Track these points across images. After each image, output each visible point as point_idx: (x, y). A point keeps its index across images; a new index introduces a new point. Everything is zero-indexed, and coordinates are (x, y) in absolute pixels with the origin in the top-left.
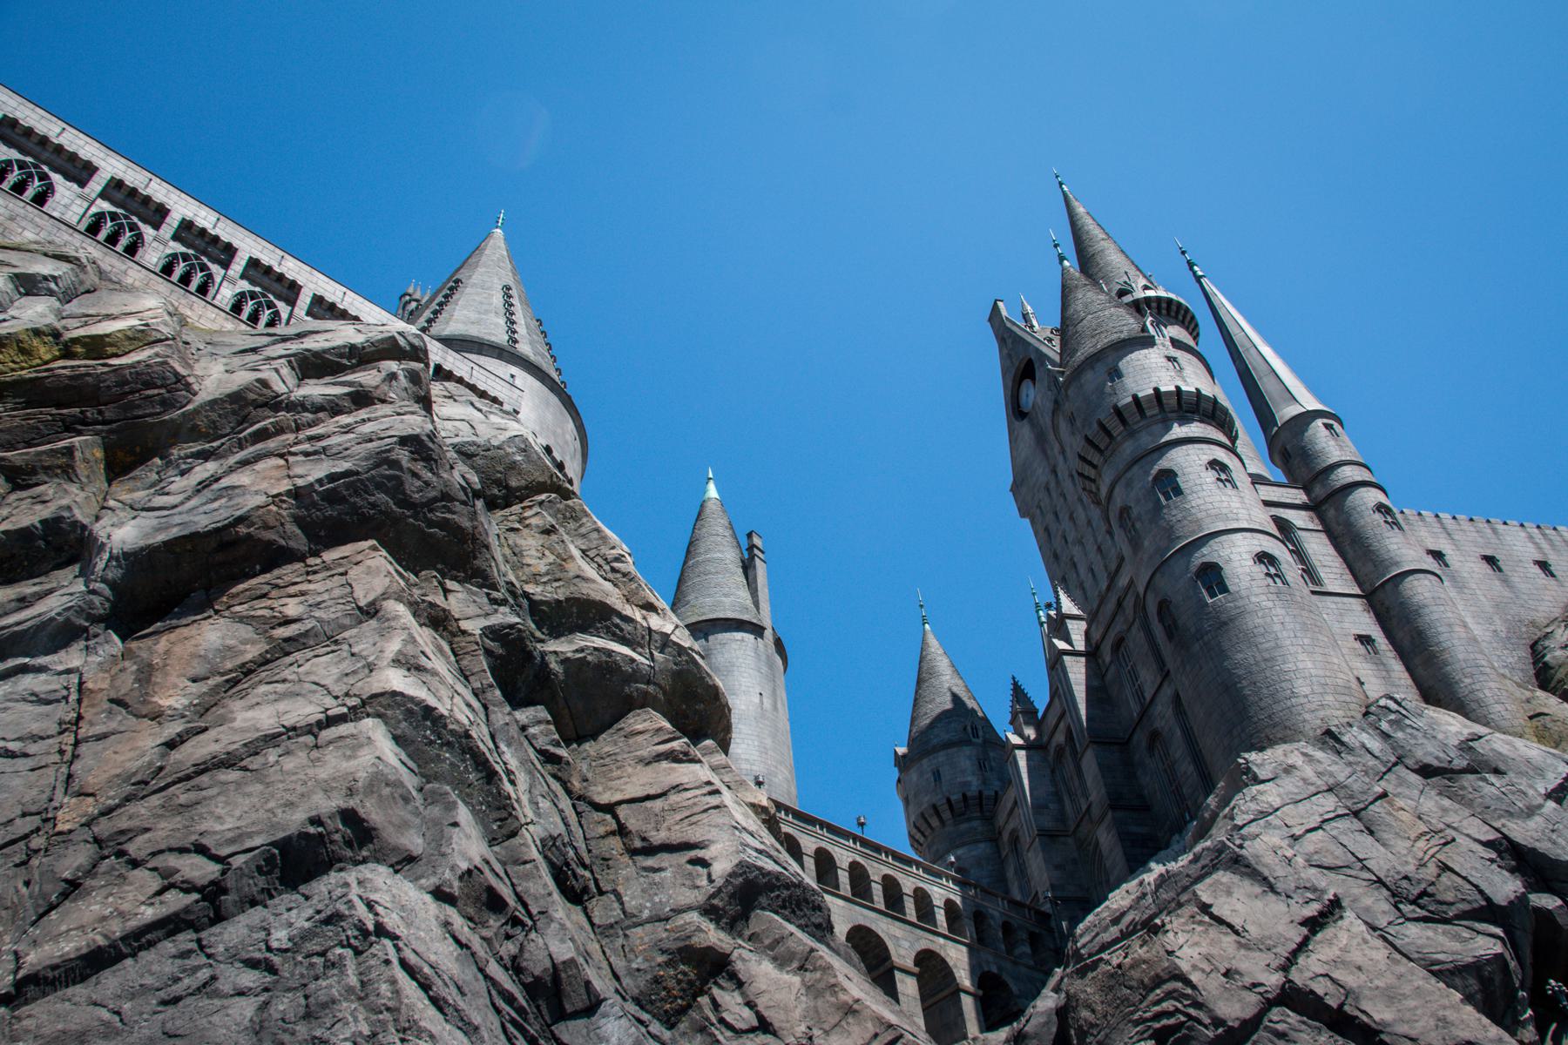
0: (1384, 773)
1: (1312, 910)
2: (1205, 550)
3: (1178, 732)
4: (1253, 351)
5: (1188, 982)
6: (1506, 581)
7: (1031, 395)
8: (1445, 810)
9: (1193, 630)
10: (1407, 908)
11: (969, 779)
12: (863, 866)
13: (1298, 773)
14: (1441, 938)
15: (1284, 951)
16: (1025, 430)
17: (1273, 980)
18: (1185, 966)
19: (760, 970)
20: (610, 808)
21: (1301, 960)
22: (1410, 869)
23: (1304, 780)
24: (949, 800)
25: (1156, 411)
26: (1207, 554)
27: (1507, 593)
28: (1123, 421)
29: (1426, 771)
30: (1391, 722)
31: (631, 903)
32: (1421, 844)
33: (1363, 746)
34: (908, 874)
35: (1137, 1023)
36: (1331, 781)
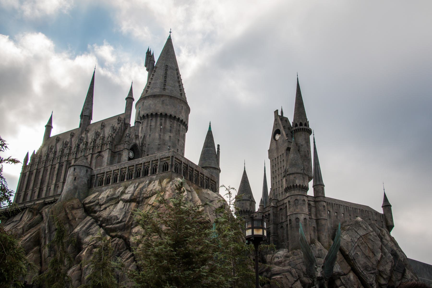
1: (296, 279)
3: (286, 230)
5: (283, 284)
7: (277, 137)
9: (293, 226)
10: (305, 275)
11: (248, 207)
14: (307, 280)
15: (292, 283)
17: (291, 286)
18: (283, 283)
21: (293, 285)
23: (300, 256)
24: (244, 210)
28: (294, 187)
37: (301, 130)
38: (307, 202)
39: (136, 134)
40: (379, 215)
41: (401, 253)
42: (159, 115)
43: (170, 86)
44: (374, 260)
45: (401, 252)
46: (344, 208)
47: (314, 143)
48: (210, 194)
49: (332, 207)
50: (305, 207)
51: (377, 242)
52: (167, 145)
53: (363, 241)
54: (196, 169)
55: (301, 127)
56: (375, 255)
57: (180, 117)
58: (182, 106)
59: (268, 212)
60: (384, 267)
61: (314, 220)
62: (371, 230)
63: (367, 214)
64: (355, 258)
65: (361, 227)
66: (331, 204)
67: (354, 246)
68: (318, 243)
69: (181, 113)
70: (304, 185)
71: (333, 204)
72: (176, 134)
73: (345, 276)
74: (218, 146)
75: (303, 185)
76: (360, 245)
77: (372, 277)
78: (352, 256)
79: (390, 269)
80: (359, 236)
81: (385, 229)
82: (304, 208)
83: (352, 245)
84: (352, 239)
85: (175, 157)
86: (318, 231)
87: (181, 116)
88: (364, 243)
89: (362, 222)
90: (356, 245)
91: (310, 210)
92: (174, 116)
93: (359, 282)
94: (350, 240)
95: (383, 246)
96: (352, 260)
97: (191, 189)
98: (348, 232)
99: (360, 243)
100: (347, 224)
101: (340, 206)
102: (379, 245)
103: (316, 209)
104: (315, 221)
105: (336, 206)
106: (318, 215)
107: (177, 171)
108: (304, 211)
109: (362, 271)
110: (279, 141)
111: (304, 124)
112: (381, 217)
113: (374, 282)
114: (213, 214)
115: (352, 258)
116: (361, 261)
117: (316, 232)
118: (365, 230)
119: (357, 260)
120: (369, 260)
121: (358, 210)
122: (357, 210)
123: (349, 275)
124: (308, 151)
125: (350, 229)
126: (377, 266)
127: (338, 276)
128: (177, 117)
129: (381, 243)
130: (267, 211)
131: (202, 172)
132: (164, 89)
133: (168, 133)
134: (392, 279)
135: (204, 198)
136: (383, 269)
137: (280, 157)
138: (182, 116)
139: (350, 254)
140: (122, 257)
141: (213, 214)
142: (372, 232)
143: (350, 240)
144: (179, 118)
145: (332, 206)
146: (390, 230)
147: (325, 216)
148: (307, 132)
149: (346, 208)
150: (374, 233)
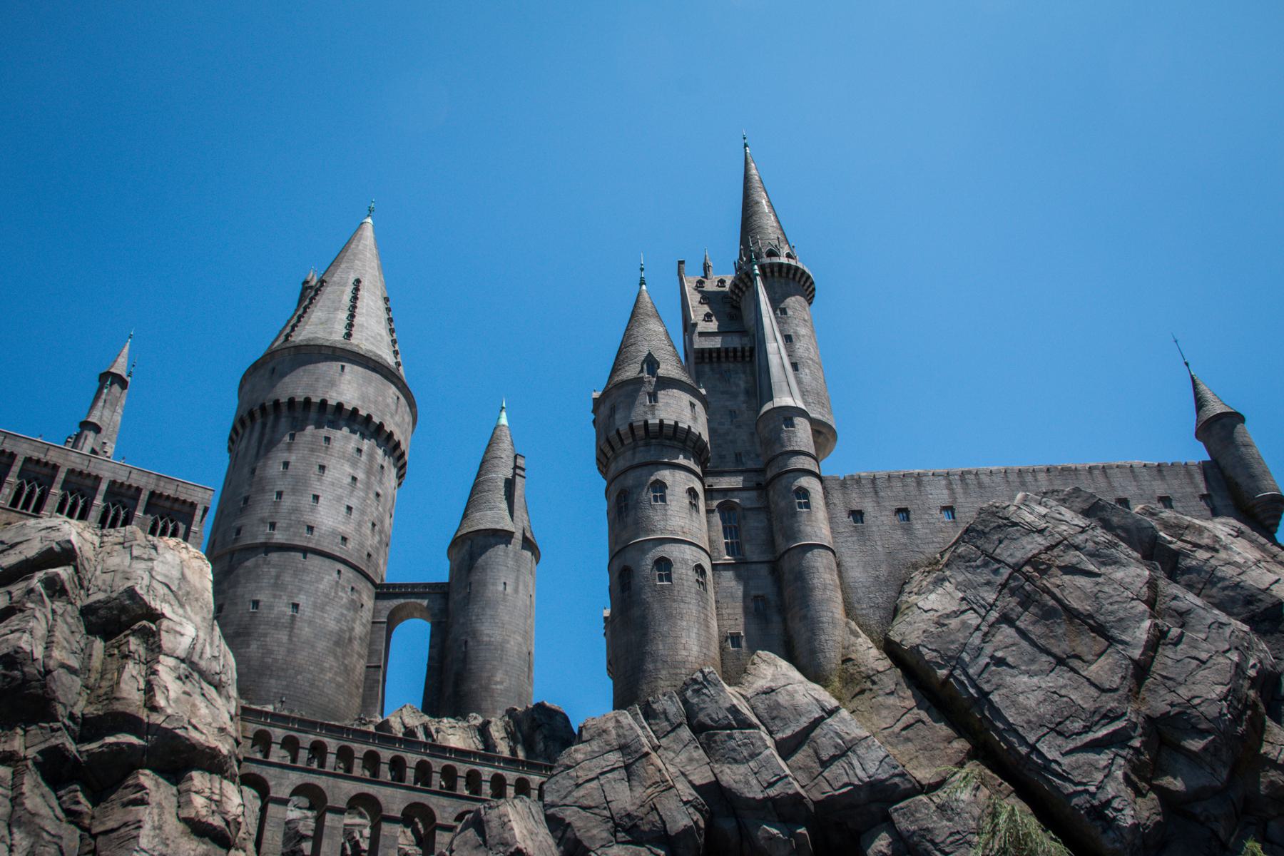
0: (669, 732)
6: (908, 530)
12: (429, 763)
13: (605, 736)
22: (630, 808)
30: (694, 691)
32: (649, 791)
33: (665, 712)
36: (623, 741)
42: (258, 411)
49: (876, 493)
57: (327, 397)
60: (1182, 691)
61: (759, 566)
62: (1076, 522)
64: (986, 687)
65: (1015, 524)
67: (978, 628)
70: (650, 422)
75: (646, 422)
77: (1103, 763)
79: (1219, 690)
80: (1006, 572)
84: (970, 594)
86: (782, 610)
90: (994, 615)
92: (302, 399)
94: (953, 606)
103: (769, 520)
104: (764, 570)
105: (897, 484)
106: (779, 540)
108: (660, 525)
109: (1033, 748)
113: (1115, 788)
117: (776, 619)
118: (1041, 532)
119: (1003, 691)
120: (1076, 672)
125: (959, 556)
126: (1134, 695)
127: (874, 808)
128: (316, 400)
129: (1147, 573)
133: (280, 454)
134: (1265, 748)
136: (1177, 700)
139: (957, 672)
142: (1083, 531)
144: (324, 403)
146: (1268, 522)
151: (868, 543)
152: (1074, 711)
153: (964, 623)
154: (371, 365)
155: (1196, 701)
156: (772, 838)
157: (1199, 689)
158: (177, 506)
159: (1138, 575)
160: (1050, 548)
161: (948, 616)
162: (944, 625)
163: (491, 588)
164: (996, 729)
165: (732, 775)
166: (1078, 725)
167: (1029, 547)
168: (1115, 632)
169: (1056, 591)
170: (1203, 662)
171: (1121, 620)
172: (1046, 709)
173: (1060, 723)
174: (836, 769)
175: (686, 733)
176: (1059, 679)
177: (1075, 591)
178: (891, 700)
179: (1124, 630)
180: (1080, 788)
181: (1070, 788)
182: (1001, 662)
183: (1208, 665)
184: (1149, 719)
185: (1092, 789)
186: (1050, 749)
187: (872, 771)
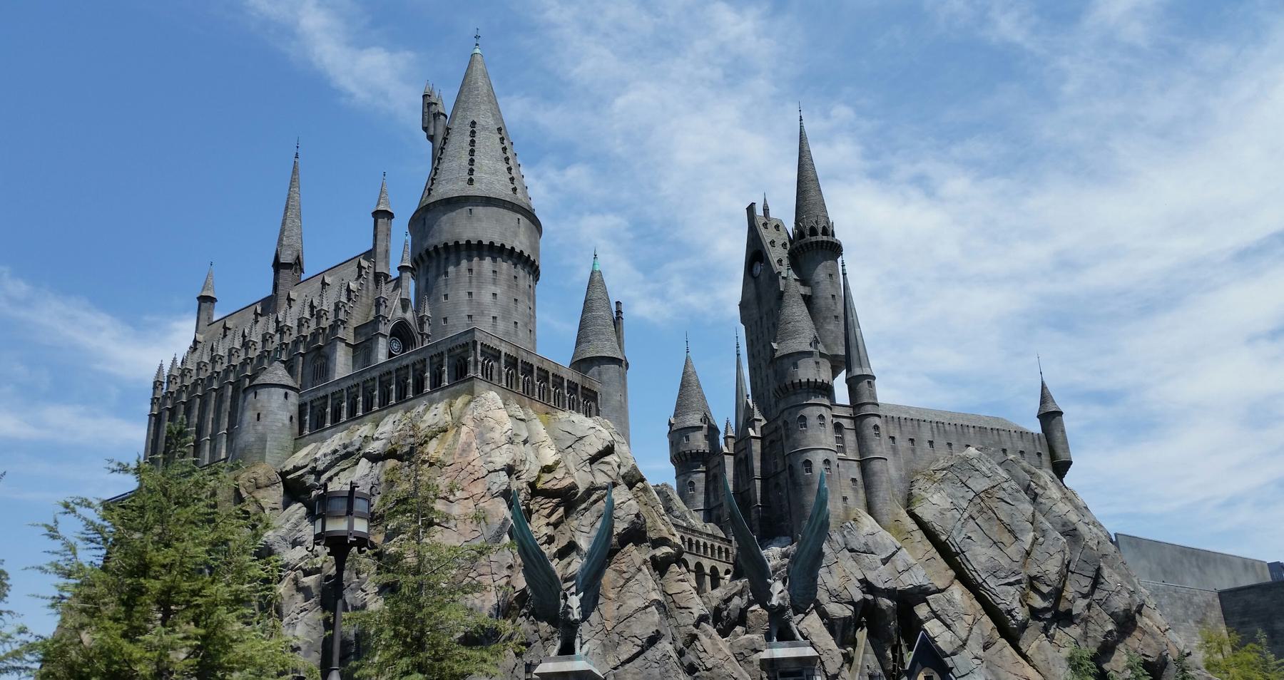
2: (808, 454)
4: (853, 330)
6: (913, 451)
8: (852, 566)
11: (700, 444)
14: (838, 609)
16: (752, 285)
19: (702, 637)
20: (671, 595)
21: (801, 623)
22: (835, 587)
25: (806, 387)
26: (809, 456)
27: (913, 457)
29: (852, 550)
31: (679, 622)
32: (842, 580)
34: (694, 536)
35: (763, 629)
37: (814, 245)
38: (829, 418)
39: (402, 297)
40: (1031, 438)
41: (1090, 529)
42: (464, 247)
43: (486, 174)
44: (1014, 551)
45: (1091, 526)
46: (932, 428)
47: (844, 274)
48: (576, 421)
49: (900, 428)
50: (825, 432)
51: (1021, 507)
52: (489, 315)
53: (982, 504)
54: (541, 366)
55: (814, 239)
56: (1016, 538)
58: (519, 219)
59: (744, 451)
63: (997, 437)
66: (896, 420)
68: (866, 517)
69: (516, 235)
71: (902, 421)
72: (509, 287)
73: (939, 595)
74: (618, 303)
75: (816, 380)
76: (975, 515)
77: (1012, 593)
78: (955, 544)
79: (1057, 569)
81: (1047, 473)
82: (823, 436)
83: (956, 518)
84: (955, 502)
85: (482, 344)
87: (518, 243)
88: (985, 510)
89: (979, 459)
90: (966, 515)
91: (840, 439)
93: (978, 606)
94: (948, 506)
95: (1037, 514)
96: (957, 554)
97: (525, 414)
98: (942, 486)
99: (975, 511)
100: (940, 467)
101: (922, 423)
102: (1026, 513)
105: (909, 423)
107: (489, 376)
108: (824, 441)
109: (984, 581)
110: (762, 278)
111: (820, 231)
112: (1034, 441)
113: (1016, 604)
114: (585, 468)
115: (958, 549)
116: (979, 556)
119: (970, 552)
120: (1002, 550)
121: (971, 430)
122: (968, 430)
123: (950, 592)
124: (833, 296)
125: (948, 479)
127: (920, 595)
128: (508, 247)
130: (743, 450)
131: (556, 372)
132: (471, 181)
133: (489, 287)
135: (562, 432)
136: (1041, 571)
137: (765, 316)
138: (520, 242)
139: (950, 539)
140: (366, 592)
141: (583, 468)
143: (948, 506)
145: (900, 424)
147: (879, 449)
148: (830, 249)
149: (937, 426)
150: (1013, 482)
151: (898, 456)
152: (1001, 569)
153: (953, 515)
154: (531, 218)
155: (1047, 572)
156: (888, 606)
157: (1049, 567)
158: (589, 394)
159: (1029, 509)
160: (994, 487)
161: (945, 510)
162: (944, 514)
163: (615, 397)
164: (968, 569)
165: (871, 577)
166: (1003, 575)
167: (984, 484)
168: (1018, 535)
169: (994, 509)
170: (1051, 555)
171: (1021, 530)
172: (989, 564)
173: (995, 572)
174: (905, 576)
175: (848, 553)
176: (994, 552)
177: (1003, 511)
178: (920, 545)
179: (1022, 535)
180: (1004, 602)
181: (999, 601)
182: (969, 538)
183: (1053, 557)
184: (1029, 576)
185: (1008, 603)
186: (992, 583)
187: (921, 581)
